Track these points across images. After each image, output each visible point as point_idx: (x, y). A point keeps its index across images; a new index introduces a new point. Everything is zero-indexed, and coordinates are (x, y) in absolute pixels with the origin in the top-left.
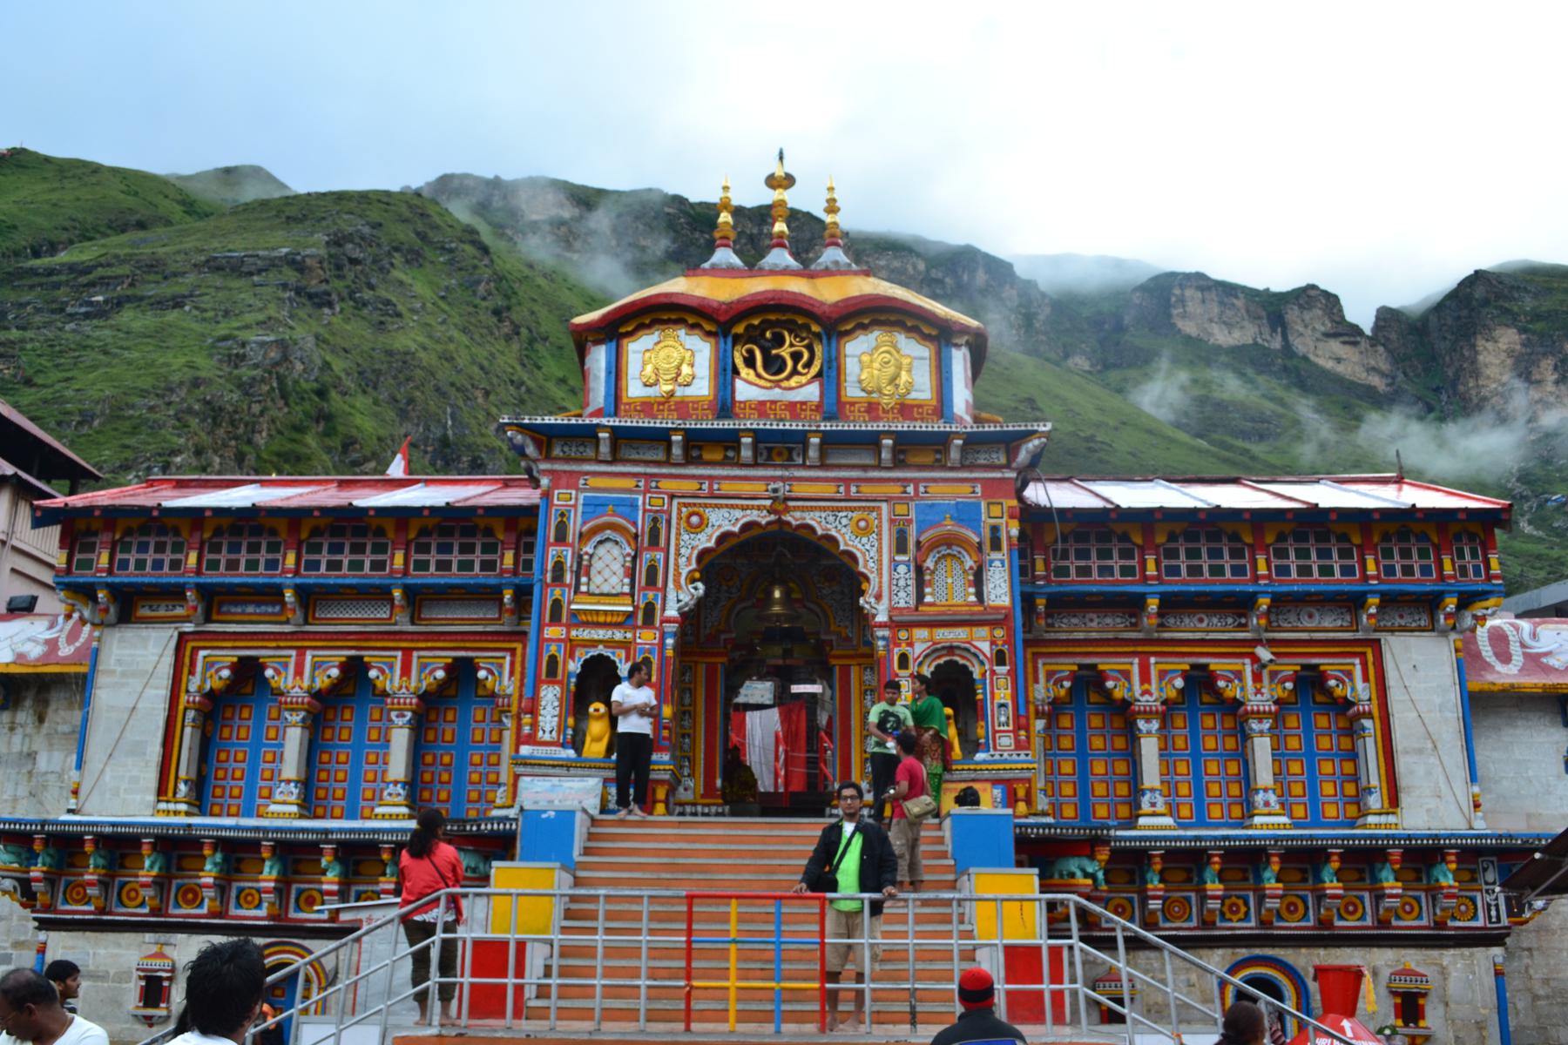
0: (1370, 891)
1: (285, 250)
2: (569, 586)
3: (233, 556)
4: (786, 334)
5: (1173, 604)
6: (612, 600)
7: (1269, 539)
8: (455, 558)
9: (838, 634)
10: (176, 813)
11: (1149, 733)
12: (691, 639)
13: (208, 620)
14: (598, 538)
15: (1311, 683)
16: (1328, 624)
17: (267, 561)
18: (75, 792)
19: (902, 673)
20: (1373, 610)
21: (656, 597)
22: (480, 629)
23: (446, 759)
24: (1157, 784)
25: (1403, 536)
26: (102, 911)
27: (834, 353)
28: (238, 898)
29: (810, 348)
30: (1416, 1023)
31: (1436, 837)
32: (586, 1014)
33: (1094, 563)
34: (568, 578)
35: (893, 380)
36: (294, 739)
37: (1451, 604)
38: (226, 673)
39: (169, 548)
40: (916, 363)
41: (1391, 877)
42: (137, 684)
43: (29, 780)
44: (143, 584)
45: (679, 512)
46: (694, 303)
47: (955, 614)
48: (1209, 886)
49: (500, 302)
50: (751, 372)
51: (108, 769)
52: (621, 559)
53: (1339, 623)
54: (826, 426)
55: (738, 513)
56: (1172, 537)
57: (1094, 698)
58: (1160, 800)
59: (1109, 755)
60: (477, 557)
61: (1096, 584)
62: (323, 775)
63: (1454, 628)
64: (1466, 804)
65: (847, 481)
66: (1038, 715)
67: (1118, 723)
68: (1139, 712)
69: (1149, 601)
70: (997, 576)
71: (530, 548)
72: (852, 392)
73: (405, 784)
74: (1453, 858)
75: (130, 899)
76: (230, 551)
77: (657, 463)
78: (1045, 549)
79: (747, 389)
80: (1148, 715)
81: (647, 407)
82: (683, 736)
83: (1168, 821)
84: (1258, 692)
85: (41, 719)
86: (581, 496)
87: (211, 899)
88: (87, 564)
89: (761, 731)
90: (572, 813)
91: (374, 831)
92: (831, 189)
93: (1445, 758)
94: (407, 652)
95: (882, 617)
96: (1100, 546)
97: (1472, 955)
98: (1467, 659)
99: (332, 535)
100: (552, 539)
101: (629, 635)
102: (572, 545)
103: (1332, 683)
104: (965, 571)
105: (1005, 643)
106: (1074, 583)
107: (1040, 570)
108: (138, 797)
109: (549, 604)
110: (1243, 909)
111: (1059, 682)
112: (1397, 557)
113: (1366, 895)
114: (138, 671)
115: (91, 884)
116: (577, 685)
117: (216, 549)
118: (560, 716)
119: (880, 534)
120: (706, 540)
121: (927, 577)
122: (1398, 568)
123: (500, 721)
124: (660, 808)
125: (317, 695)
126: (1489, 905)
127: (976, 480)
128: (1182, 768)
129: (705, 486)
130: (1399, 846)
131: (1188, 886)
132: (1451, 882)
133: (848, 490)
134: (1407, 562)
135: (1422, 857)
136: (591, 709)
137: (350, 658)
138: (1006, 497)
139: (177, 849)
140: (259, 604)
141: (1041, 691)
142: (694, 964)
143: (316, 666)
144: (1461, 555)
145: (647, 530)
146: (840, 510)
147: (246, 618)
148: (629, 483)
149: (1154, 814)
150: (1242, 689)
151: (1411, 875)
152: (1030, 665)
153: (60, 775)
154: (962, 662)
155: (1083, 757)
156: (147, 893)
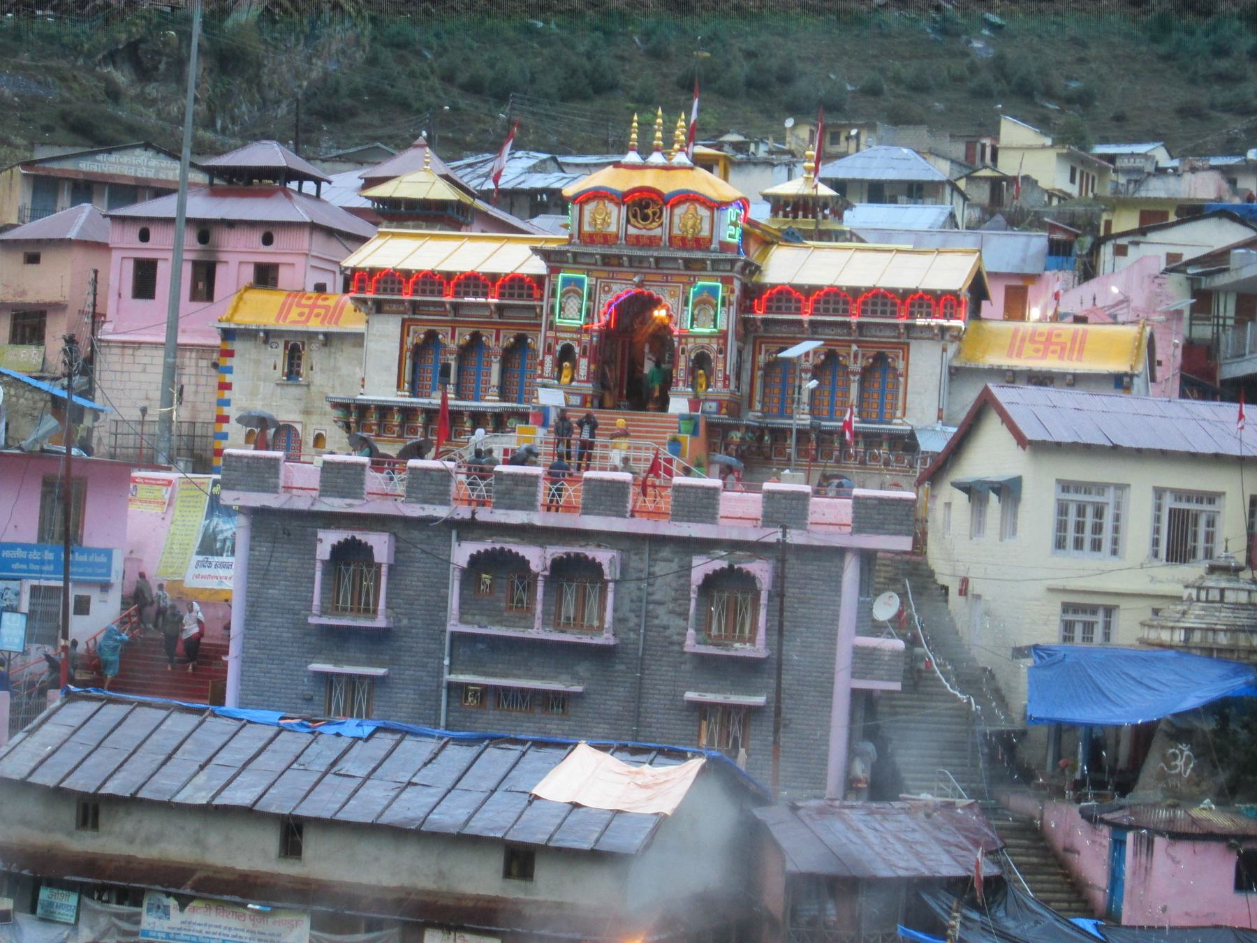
13: (414, 313)
38: (422, 336)
66: (759, 369)
80: (806, 371)
95: (676, 333)
120: (609, 298)
124: (589, 405)
139: (408, 412)
143: (460, 334)
156: (396, 429)
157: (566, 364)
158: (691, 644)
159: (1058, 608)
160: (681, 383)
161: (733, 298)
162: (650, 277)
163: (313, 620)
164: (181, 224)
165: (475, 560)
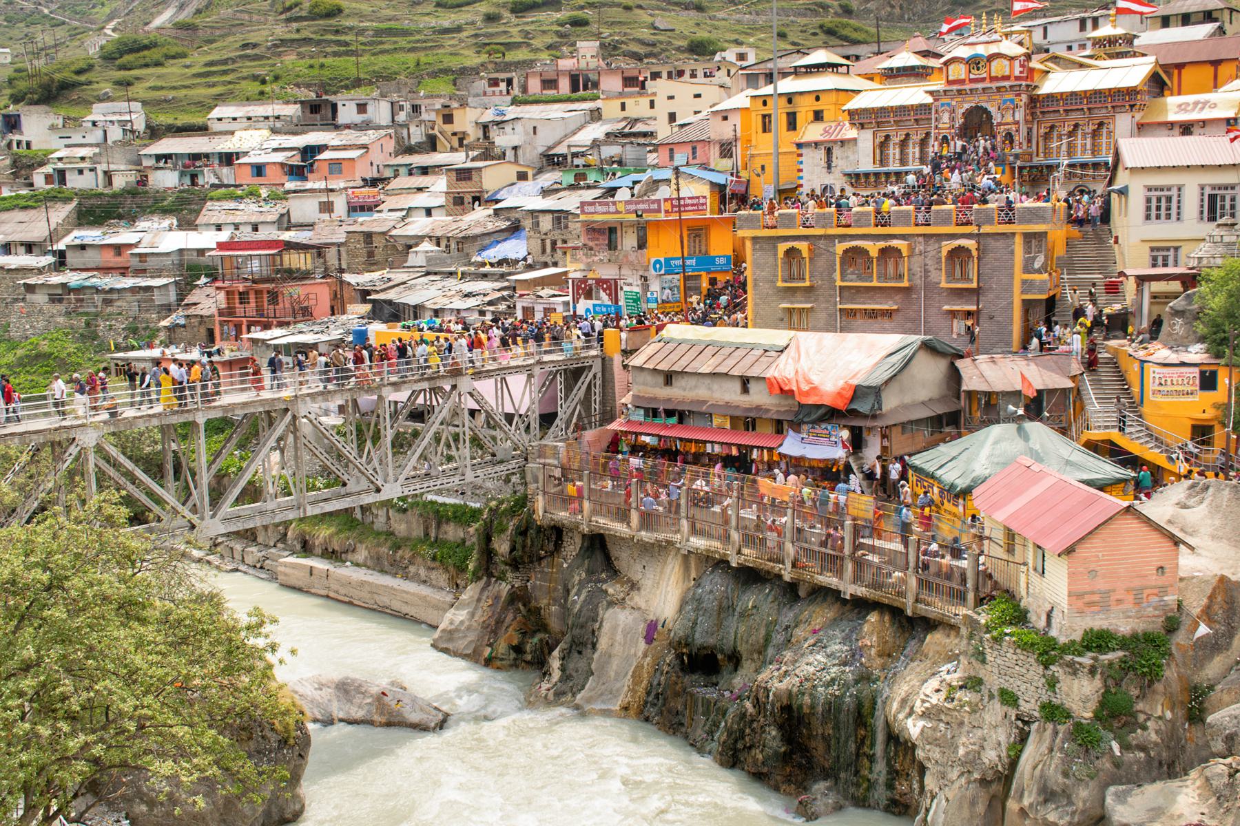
120: (963, 111)
139: (877, 175)
141: (1042, 131)
158: (944, 285)
159: (1148, 250)
161: (1022, 104)
163: (780, 284)
164: (776, 97)
165: (846, 251)
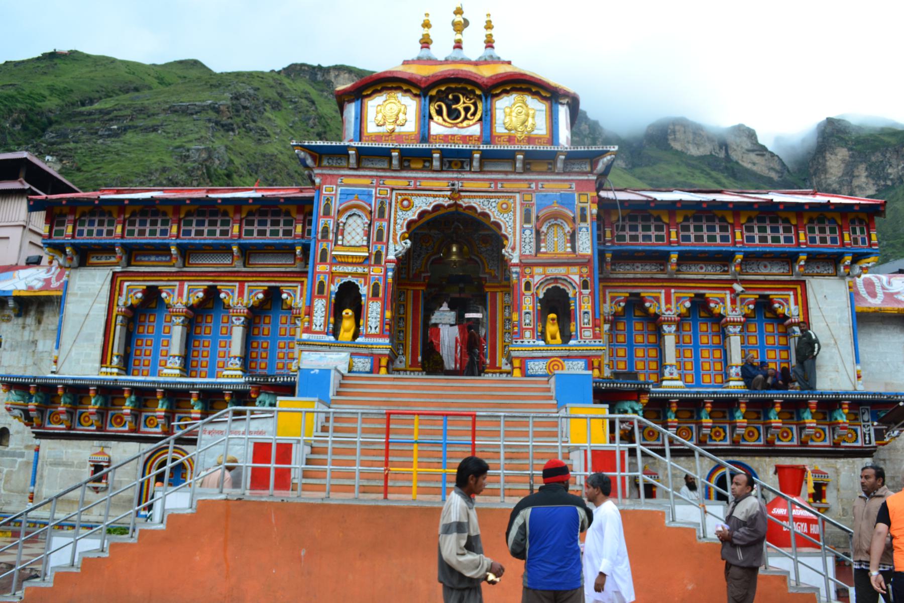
0: (797, 425)
1: (209, 102)
2: (331, 241)
3: (142, 228)
4: (461, 96)
5: (686, 258)
6: (356, 249)
7: (743, 221)
8: (268, 228)
9: (490, 274)
10: (111, 374)
11: (670, 333)
12: (404, 276)
14: (349, 213)
15: (764, 306)
16: (776, 272)
17: (161, 231)
18: (56, 362)
19: (527, 293)
20: (802, 263)
21: (382, 248)
22: (283, 270)
23: (265, 345)
24: (674, 362)
25: (821, 220)
26: (69, 428)
27: (489, 107)
28: (145, 421)
29: (475, 104)
30: (820, 500)
31: (837, 394)
32: (321, 488)
33: (640, 233)
34: (331, 236)
35: (524, 123)
36: (177, 332)
37: (848, 260)
38: (139, 295)
39: (106, 223)
40: (537, 113)
41: (810, 417)
42: (89, 301)
43: (33, 356)
44: (91, 244)
45: (397, 197)
46: (406, 77)
47: (558, 258)
48: (704, 420)
49: (321, 129)
50: (440, 118)
51: (73, 349)
52: (362, 225)
53: (782, 271)
54: (483, 147)
55: (431, 199)
56: (686, 219)
57: (638, 313)
58: (675, 372)
59: (646, 346)
60: (281, 228)
61: (641, 245)
62: (195, 354)
63: (848, 274)
64: (853, 376)
65: (496, 181)
66: (606, 322)
67: (651, 327)
68: (664, 321)
69: (672, 255)
70: (584, 237)
71: (310, 223)
72: (499, 129)
73: (240, 358)
74: (846, 406)
75: (85, 421)
76: (140, 225)
77: (384, 170)
78: (611, 225)
79: (439, 127)
80: (670, 322)
81: (378, 137)
82: (400, 332)
83: (680, 383)
84: (734, 310)
85: (39, 322)
86: (339, 189)
87: (131, 422)
88: (60, 233)
89: (448, 336)
90: (329, 371)
91: (220, 384)
92: (489, 15)
93: (841, 350)
94: (242, 283)
95: (515, 260)
96: (644, 223)
97: (853, 462)
98: (854, 295)
99: (198, 215)
100: (322, 214)
101: (366, 270)
102: (333, 218)
103: (776, 305)
104: (565, 234)
105: (588, 276)
106: (628, 245)
107: (608, 236)
108: (90, 365)
109: (319, 252)
110: (723, 434)
111: (618, 303)
112: (817, 232)
113: (794, 427)
114: (90, 293)
115: (62, 413)
116: (336, 299)
117: (132, 223)
118: (325, 317)
119: (515, 212)
120: (412, 215)
121: (542, 237)
122: (818, 239)
123: (295, 324)
125: (191, 308)
126: (865, 434)
127: (572, 180)
128: (688, 354)
129: (412, 183)
130: (815, 399)
131: (690, 421)
132: (845, 420)
133: (496, 186)
134: (822, 235)
135: (828, 406)
136: (344, 313)
137: (210, 287)
138: (590, 190)
139: (110, 394)
140: (157, 255)
141: (607, 308)
142: (390, 459)
143: (190, 291)
144: (854, 232)
145: (377, 209)
146: (491, 198)
147: (150, 264)
148: (367, 181)
149: (672, 380)
150: (724, 308)
151: (821, 416)
152: (601, 293)
153: (50, 353)
154: (562, 287)
155: (631, 346)
156: (94, 418)
157: (347, 312)
160: (528, 334)
162: (468, 186)
